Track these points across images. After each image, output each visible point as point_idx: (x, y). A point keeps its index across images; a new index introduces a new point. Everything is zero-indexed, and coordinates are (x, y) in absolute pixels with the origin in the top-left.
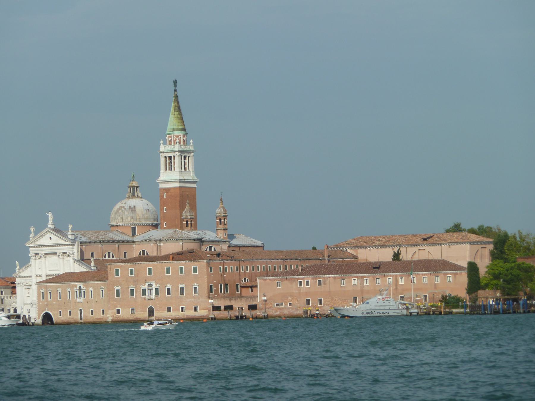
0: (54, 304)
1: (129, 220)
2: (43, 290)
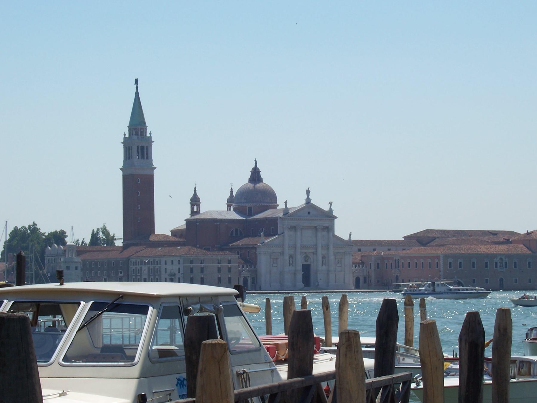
2: (450, 260)
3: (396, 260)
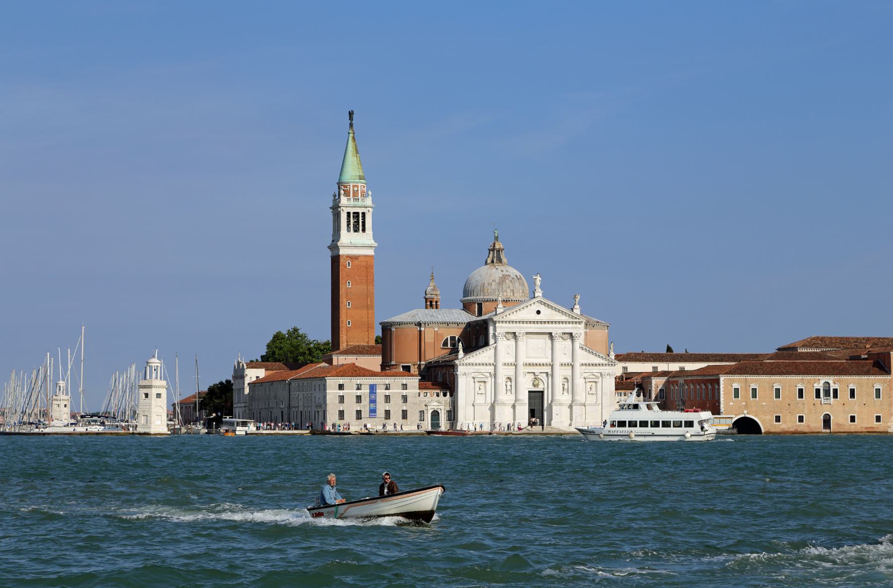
0: (763, 405)
1: (521, 295)
2: (736, 385)
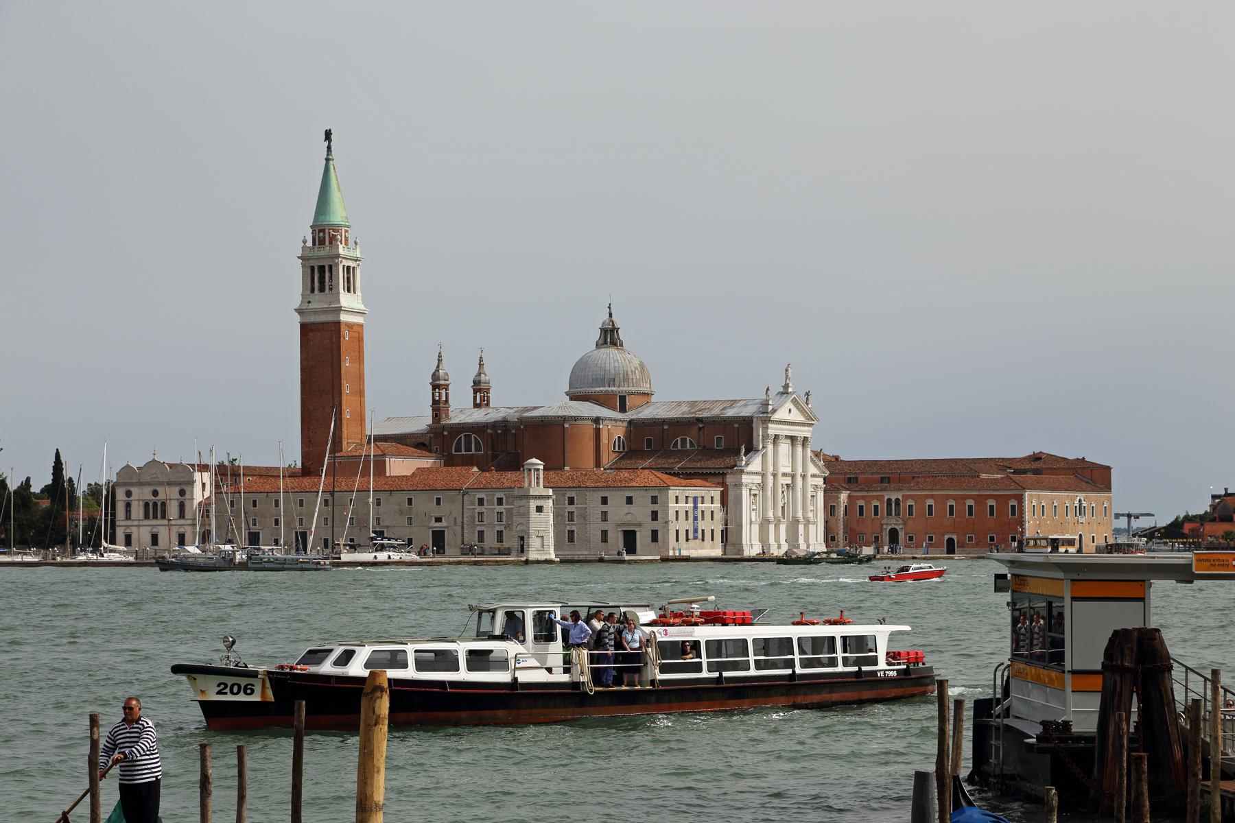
3: (889, 500)
